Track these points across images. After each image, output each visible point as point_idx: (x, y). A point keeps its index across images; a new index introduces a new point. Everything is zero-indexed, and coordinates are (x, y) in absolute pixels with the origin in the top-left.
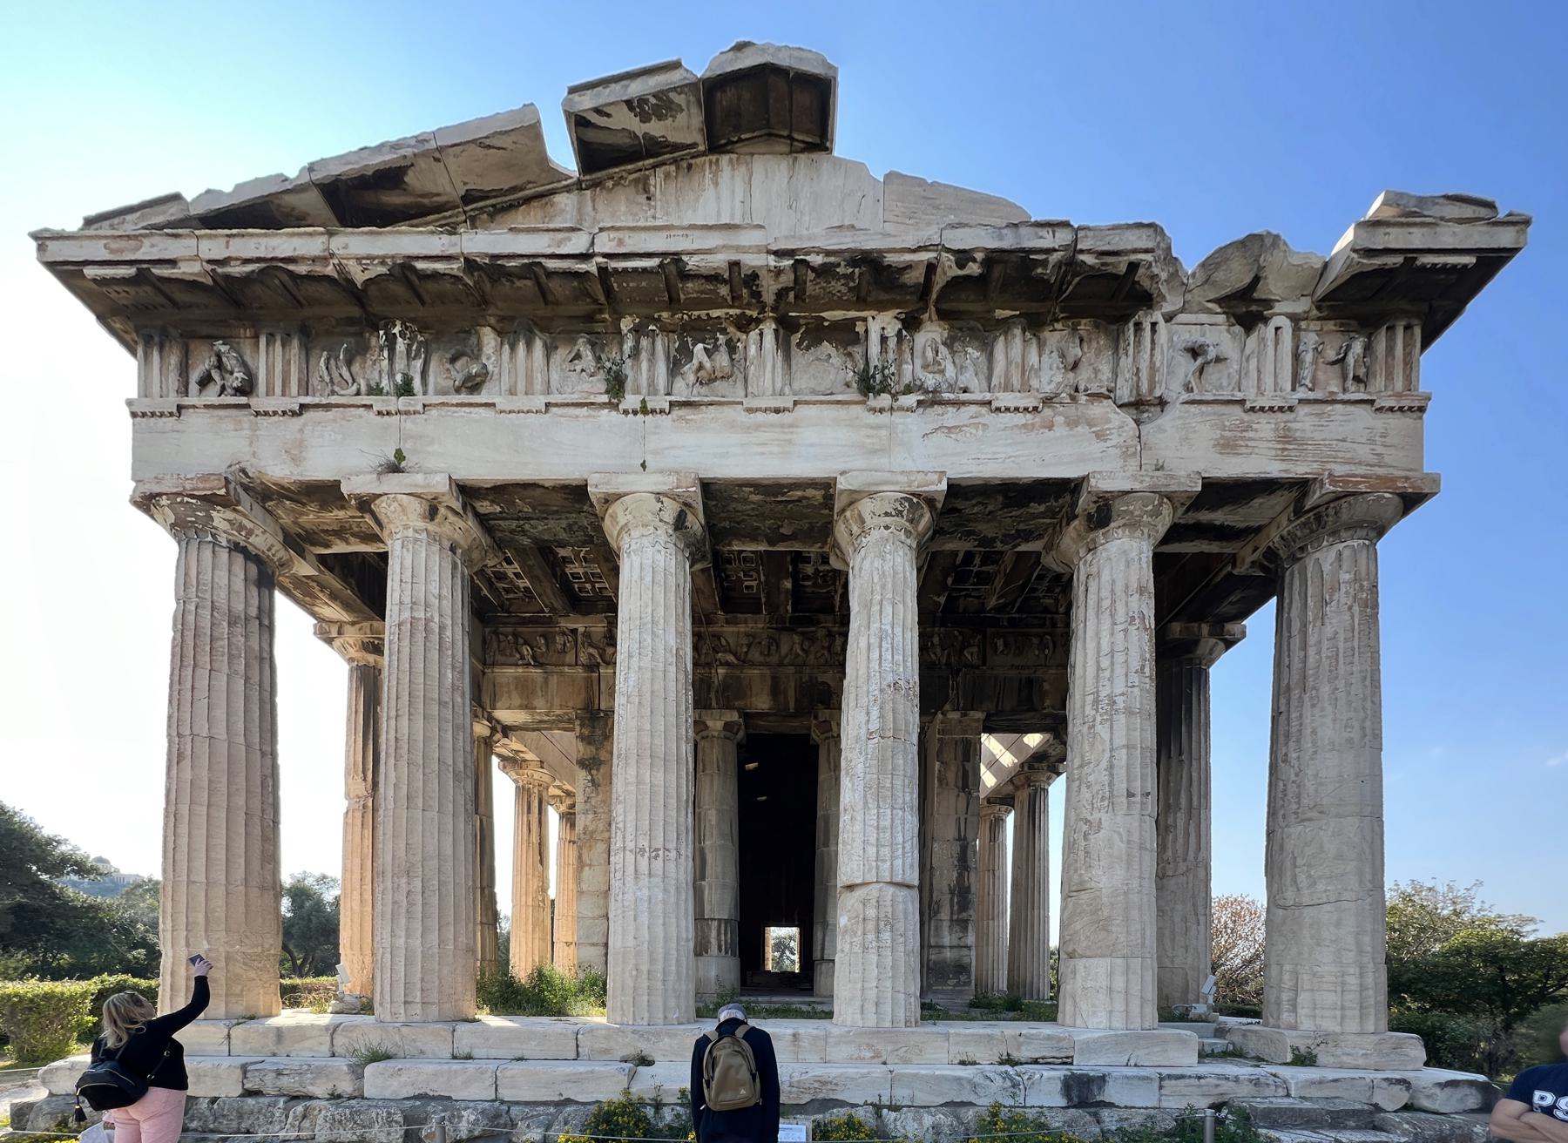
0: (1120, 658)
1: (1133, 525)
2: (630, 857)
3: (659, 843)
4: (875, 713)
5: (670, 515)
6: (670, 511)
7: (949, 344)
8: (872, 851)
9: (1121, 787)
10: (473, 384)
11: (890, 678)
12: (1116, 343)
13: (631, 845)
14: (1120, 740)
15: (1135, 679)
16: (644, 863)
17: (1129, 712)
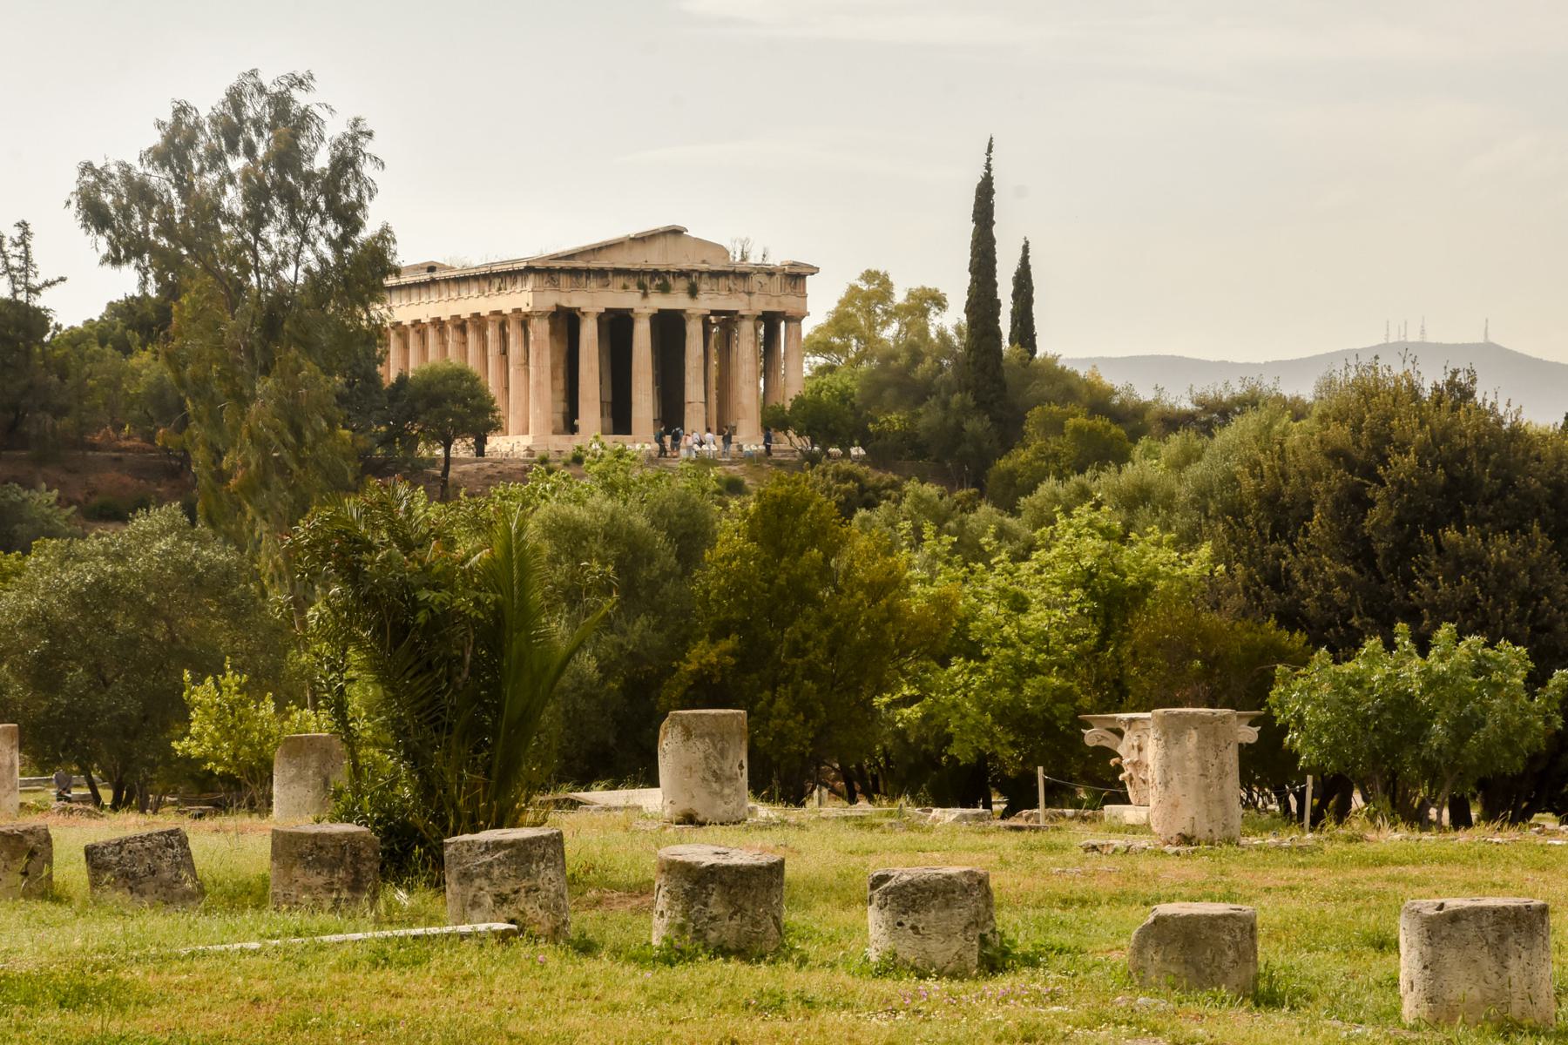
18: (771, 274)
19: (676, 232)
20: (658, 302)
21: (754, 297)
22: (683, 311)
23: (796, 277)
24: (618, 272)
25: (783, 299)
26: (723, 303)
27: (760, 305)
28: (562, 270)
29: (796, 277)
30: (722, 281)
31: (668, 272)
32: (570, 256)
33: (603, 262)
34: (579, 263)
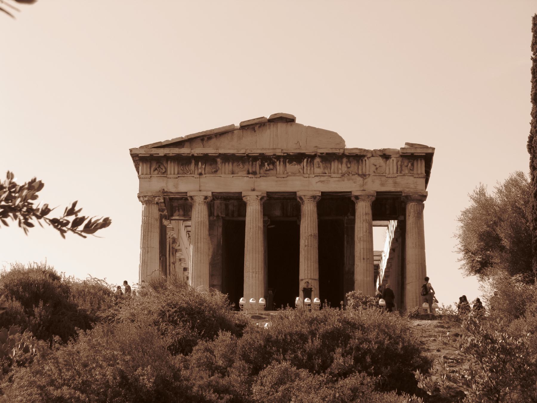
0: (362, 229)
1: (364, 200)
2: (251, 274)
3: (257, 270)
4: (306, 241)
5: (259, 199)
6: (260, 197)
7: (322, 162)
8: (306, 272)
9: (362, 258)
10: (216, 172)
11: (310, 234)
12: (358, 162)
13: (251, 271)
14: (362, 247)
15: (365, 233)
16: (254, 275)
17: (364, 241)
18: (385, 155)
19: (289, 120)
20: (270, 184)
21: (369, 180)
22: (295, 193)
23: (419, 159)
24: (227, 158)
25: (399, 180)
26: (336, 184)
27: (375, 186)
28: (167, 158)
29: (419, 159)
30: (335, 165)
31: (278, 158)
32: (179, 143)
33: (210, 150)
34: (185, 151)
